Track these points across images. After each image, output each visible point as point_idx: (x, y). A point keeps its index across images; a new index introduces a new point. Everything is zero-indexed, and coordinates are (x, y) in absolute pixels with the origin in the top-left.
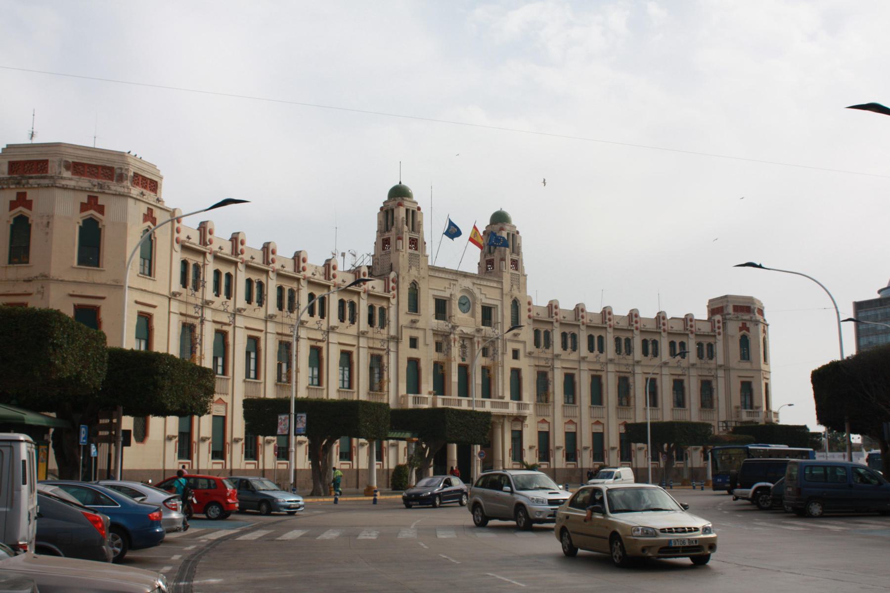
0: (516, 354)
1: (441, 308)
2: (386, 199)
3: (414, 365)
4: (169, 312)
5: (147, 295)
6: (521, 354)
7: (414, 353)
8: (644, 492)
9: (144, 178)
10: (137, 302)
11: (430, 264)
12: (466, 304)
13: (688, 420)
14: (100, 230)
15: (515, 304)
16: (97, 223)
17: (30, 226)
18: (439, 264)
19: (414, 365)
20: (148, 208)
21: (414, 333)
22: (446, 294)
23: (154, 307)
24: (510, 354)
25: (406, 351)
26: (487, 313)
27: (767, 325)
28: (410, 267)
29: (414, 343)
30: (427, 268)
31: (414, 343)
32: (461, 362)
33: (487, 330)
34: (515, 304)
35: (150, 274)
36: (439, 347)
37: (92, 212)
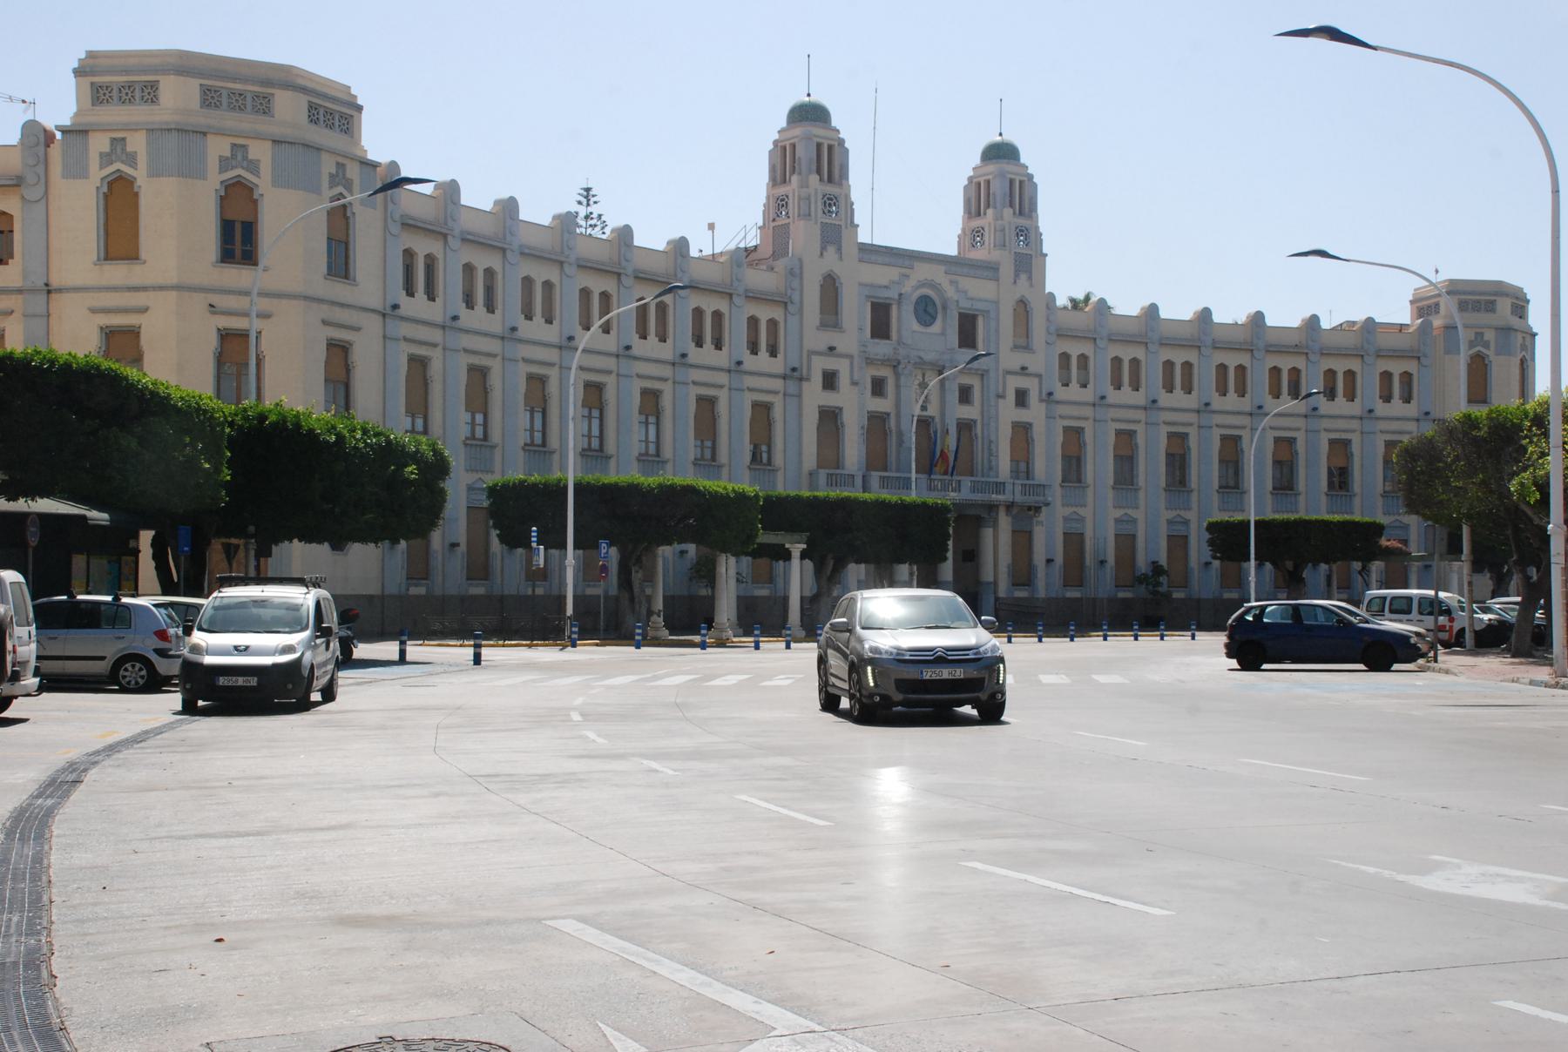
0: (1021, 398)
2: (783, 124)
3: (830, 419)
4: (385, 337)
5: (337, 309)
7: (831, 399)
8: (159, 590)
9: (329, 113)
10: (325, 322)
11: (861, 240)
12: (926, 310)
13: (1302, 514)
14: (255, 202)
15: (1023, 309)
16: (251, 190)
17: (136, 195)
18: (879, 241)
19: (830, 419)
20: (340, 166)
21: (831, 364)
22: (893, 294)
23: (358, 329)
24: (1011, 397)
25: (814, 396)
26: (967, 332)
27: (1534, 335)
28: (823, 249)
29: (830, 381)
30: (856, 251)
31: (830, 381)
34: (1023, 307)
35: (346, 277)
36: (878, 387)
37: (239, 171)
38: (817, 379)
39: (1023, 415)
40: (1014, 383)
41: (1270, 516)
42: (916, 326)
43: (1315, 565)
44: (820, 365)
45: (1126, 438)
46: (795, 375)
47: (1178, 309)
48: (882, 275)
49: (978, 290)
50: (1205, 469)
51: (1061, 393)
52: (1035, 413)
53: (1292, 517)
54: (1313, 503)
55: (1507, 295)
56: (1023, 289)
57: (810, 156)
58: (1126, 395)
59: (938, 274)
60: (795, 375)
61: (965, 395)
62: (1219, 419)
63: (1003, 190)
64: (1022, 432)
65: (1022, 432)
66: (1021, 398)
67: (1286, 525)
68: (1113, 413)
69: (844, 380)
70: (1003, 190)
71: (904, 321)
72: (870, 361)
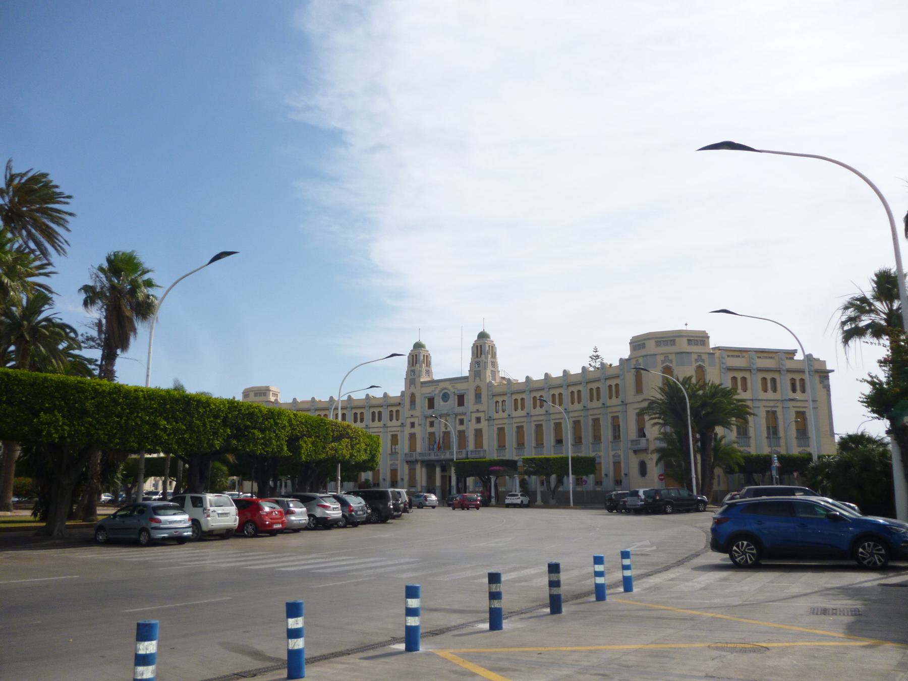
0: (478, 420)
1: (431, 403)
3: (412, 436)
6: (482, 420)
7: (413, 431)
12: (445, 397)
19: (412, 436)
21: (412, 420)
24: (474, 420)
25: (408, 430)
26: (461, 400)
29: (413, 425)
31: (413, 425)
32: (443, 429)
33: (460, 409)
36: (432, 424)
38: (408, 425)
39: (478, 426)
40: (474, 416)
41: (575, 455)
42: (442, 403)
43: (511, 477)
44: (409, 421)
45: (520, 429)
46: (403, 425)
47: (538, 376)
48: (428, 390)
49: (461, 387)
50: (549, 438)
51: (495, 416)
52: (484, 425)
53: (543, 456)
54: (549, 452)
55: (649, 339)
56: (478, 382)
57: (418, 357)
58: (520, 413)
59: (447, 385)
60: (403, 425)
61: (462, 422)
62: (534, 419)
63: (482, 349)
64: (478, 433)
65: (478, 433)
66: (478, 420)
67: (540, 460)
68: (514, 420)
69: (416, 425)
70: (482, 349)
71: (438, 402)
72: (426, 417)
